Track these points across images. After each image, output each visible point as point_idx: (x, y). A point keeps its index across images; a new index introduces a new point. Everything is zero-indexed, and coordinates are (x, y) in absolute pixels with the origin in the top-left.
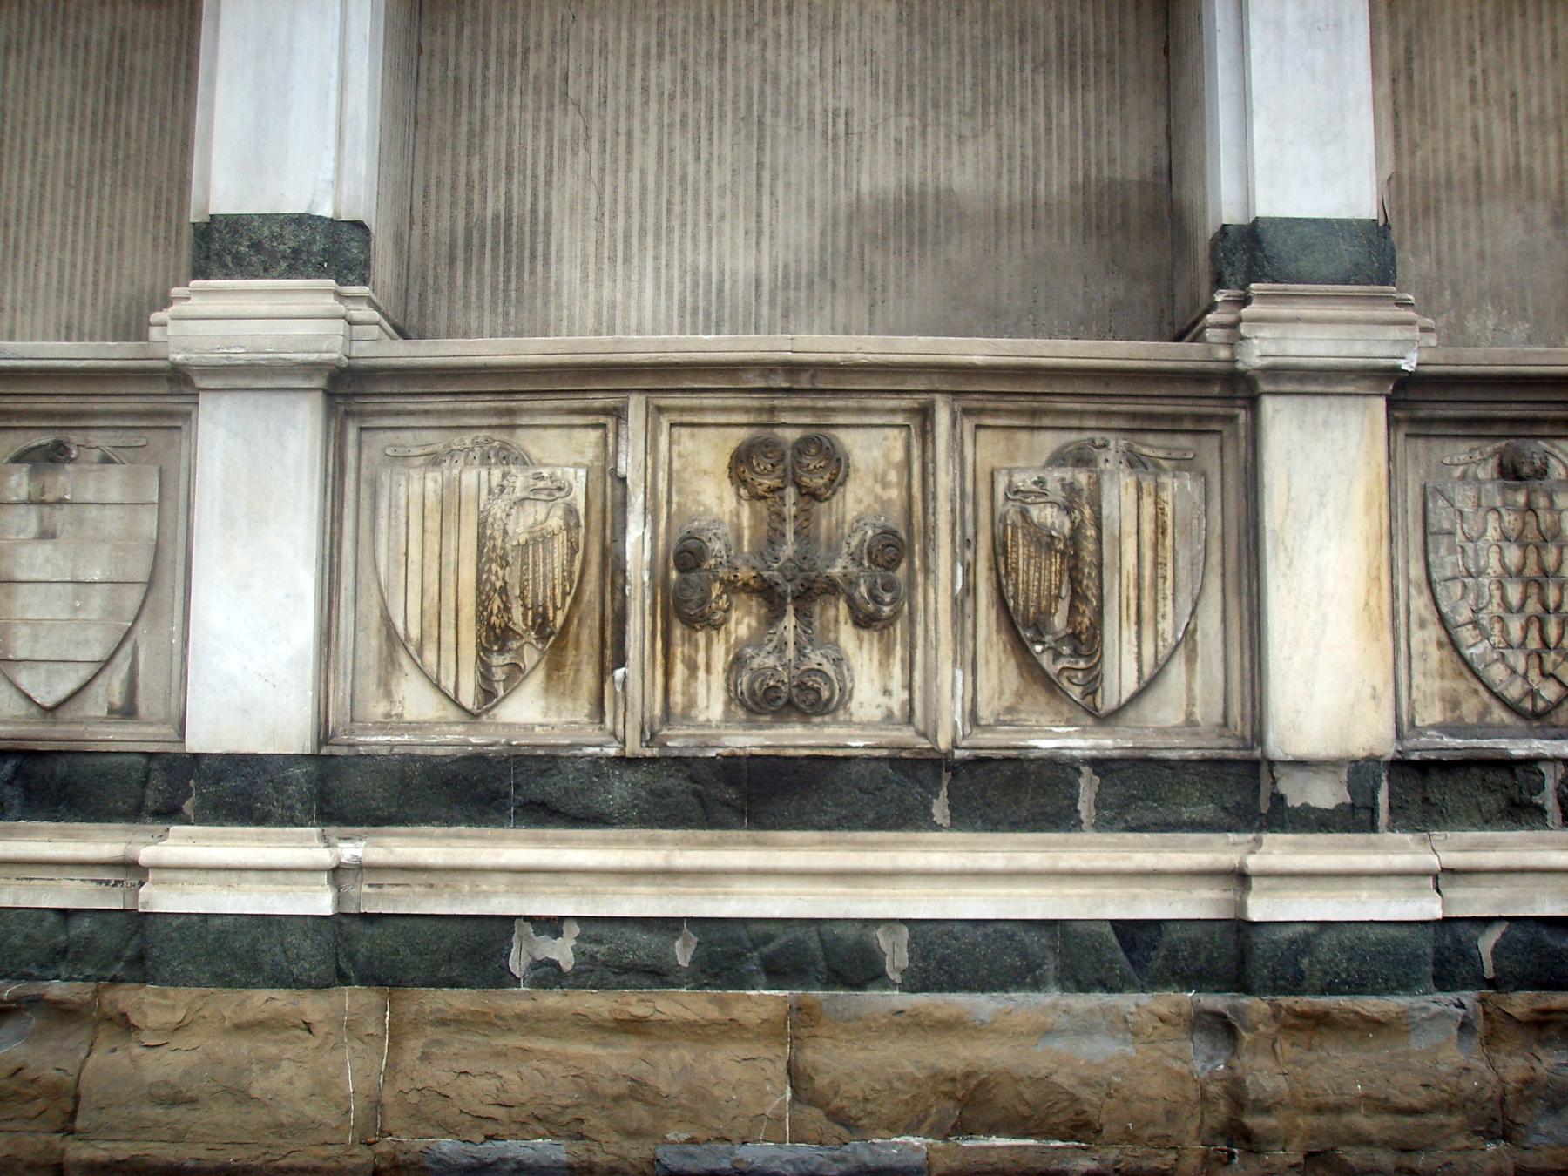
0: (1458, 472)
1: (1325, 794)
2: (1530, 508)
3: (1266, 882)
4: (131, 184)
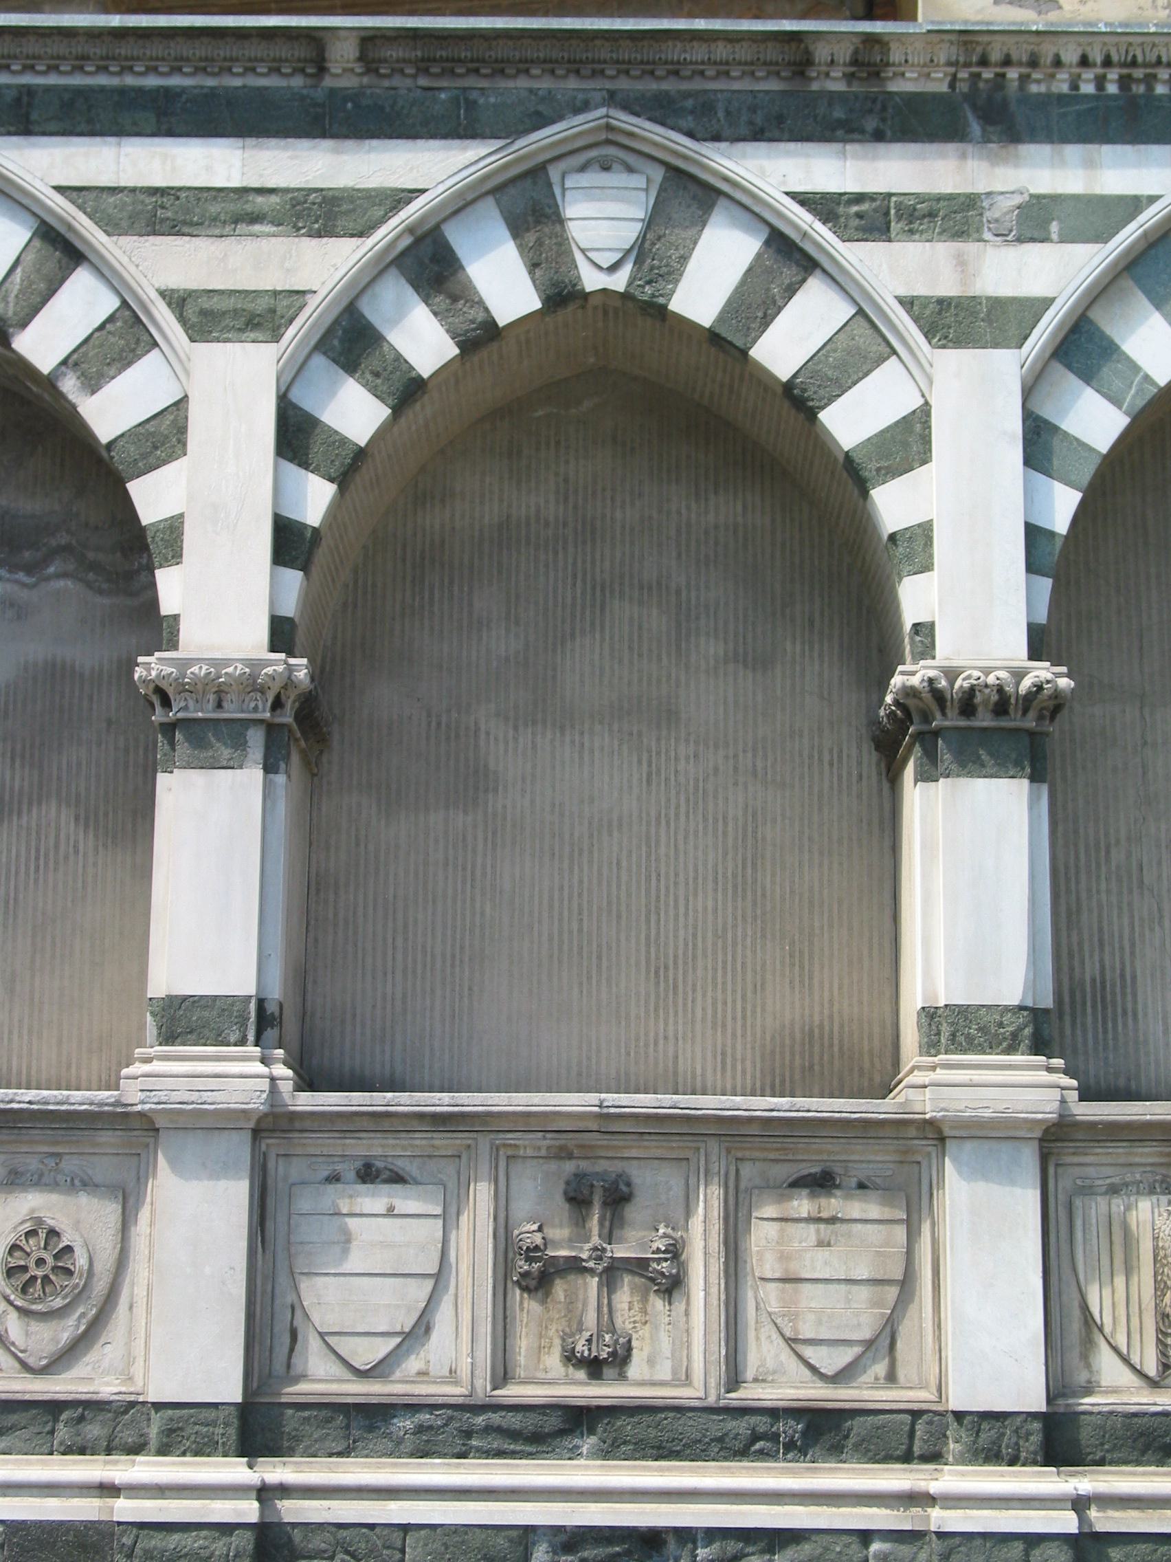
4: (769, 936)
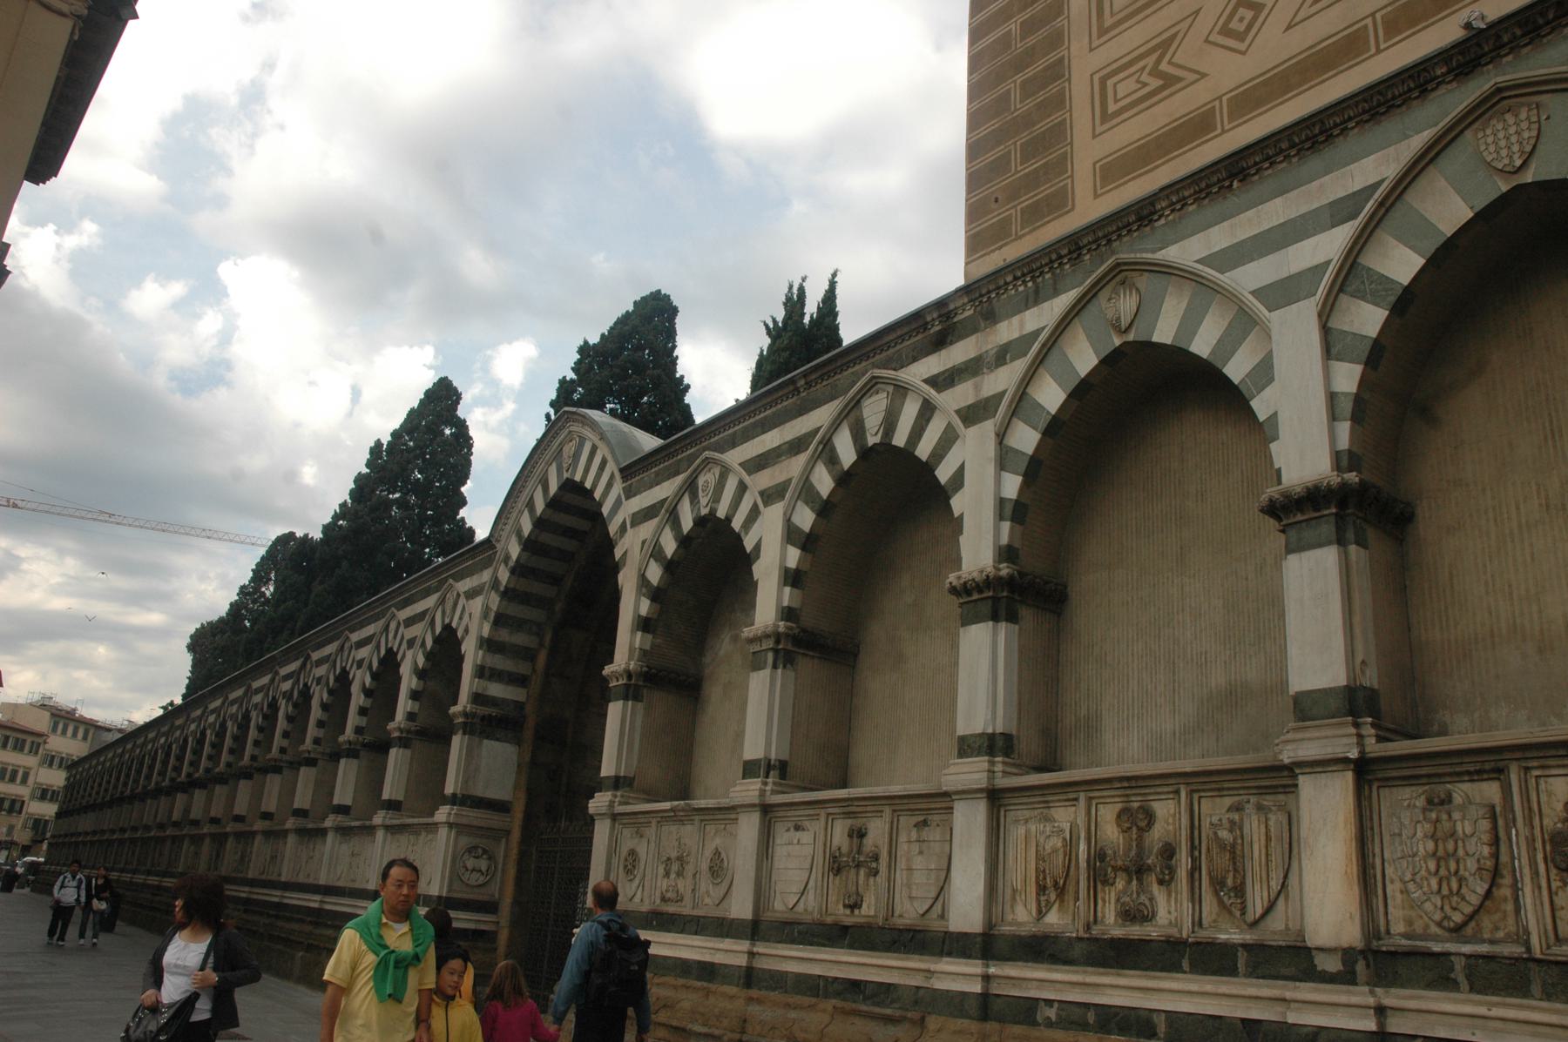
0: (1406, 804)
1: (1332, 965)
2: (1438, 820)
3: (1296, 1005)
